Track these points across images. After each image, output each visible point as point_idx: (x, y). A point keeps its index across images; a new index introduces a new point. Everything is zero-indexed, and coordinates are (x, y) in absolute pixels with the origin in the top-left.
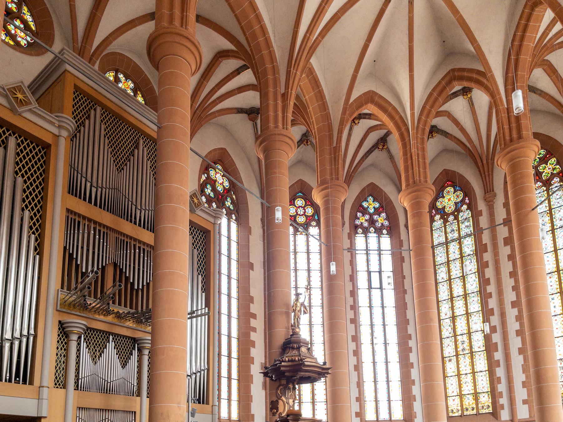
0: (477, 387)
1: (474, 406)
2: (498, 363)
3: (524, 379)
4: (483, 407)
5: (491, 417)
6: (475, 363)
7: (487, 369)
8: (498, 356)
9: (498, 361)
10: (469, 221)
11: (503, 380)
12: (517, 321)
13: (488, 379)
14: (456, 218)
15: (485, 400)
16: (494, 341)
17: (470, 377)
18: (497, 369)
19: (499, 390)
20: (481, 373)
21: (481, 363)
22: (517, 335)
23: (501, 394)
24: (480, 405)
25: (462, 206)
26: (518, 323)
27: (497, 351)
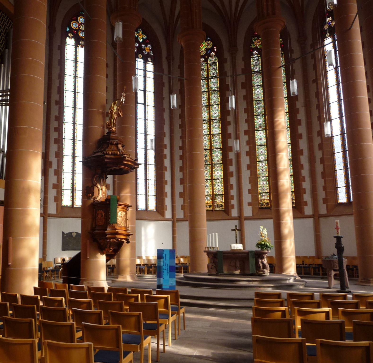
0: (214, 190)
1: (212, 204)
2: (232, 174)
5: (224, 214)
6: (214, 172)
7: (222, 177)
8: (232, 168)
10: (216, 65)
11: (235, 187)
12: (247, 145)
13: (223, 185)
14: (206, 60)
15: (219, 200)
17: (209, 182)
18: (231, 178)
19: (232, 194)
20: (218, 180)
21: (219, 173)
22: (247, 155)
23: (232, 196)
24: (215, 204)
26: (248, 147)
27: (232, 165)
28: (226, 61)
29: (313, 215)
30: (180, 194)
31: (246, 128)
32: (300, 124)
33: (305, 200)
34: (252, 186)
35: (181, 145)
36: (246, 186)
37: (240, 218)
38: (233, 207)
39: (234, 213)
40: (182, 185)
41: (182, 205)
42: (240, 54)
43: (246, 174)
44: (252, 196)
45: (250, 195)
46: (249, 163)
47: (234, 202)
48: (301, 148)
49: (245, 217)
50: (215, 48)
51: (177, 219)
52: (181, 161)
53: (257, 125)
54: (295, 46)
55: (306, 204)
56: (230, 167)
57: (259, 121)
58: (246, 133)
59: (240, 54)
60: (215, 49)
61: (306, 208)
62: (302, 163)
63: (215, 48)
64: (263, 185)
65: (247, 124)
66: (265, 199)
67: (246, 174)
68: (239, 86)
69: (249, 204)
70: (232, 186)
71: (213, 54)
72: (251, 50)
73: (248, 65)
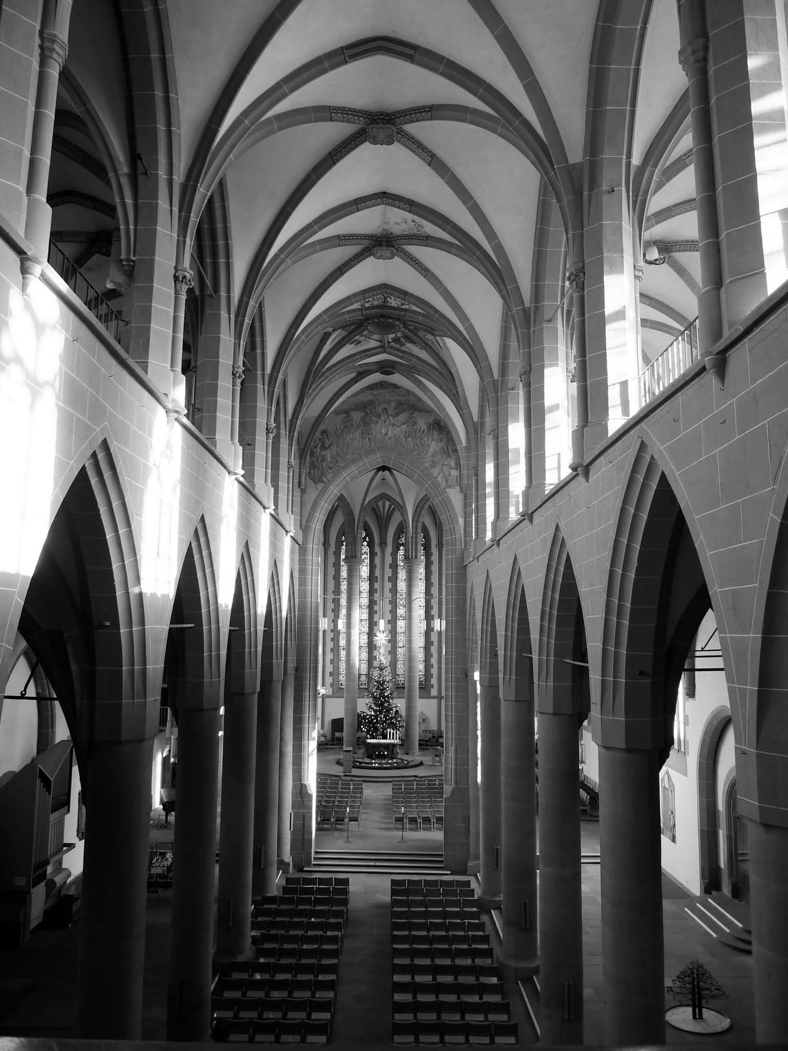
15: (363, 678)
42: (389, 549)
53: (398, 615)
54: (434, 550)
55: (432, 686)
59: (389, 549)
68: (386, 579)
71: (365, 543)
73: (395, 560)
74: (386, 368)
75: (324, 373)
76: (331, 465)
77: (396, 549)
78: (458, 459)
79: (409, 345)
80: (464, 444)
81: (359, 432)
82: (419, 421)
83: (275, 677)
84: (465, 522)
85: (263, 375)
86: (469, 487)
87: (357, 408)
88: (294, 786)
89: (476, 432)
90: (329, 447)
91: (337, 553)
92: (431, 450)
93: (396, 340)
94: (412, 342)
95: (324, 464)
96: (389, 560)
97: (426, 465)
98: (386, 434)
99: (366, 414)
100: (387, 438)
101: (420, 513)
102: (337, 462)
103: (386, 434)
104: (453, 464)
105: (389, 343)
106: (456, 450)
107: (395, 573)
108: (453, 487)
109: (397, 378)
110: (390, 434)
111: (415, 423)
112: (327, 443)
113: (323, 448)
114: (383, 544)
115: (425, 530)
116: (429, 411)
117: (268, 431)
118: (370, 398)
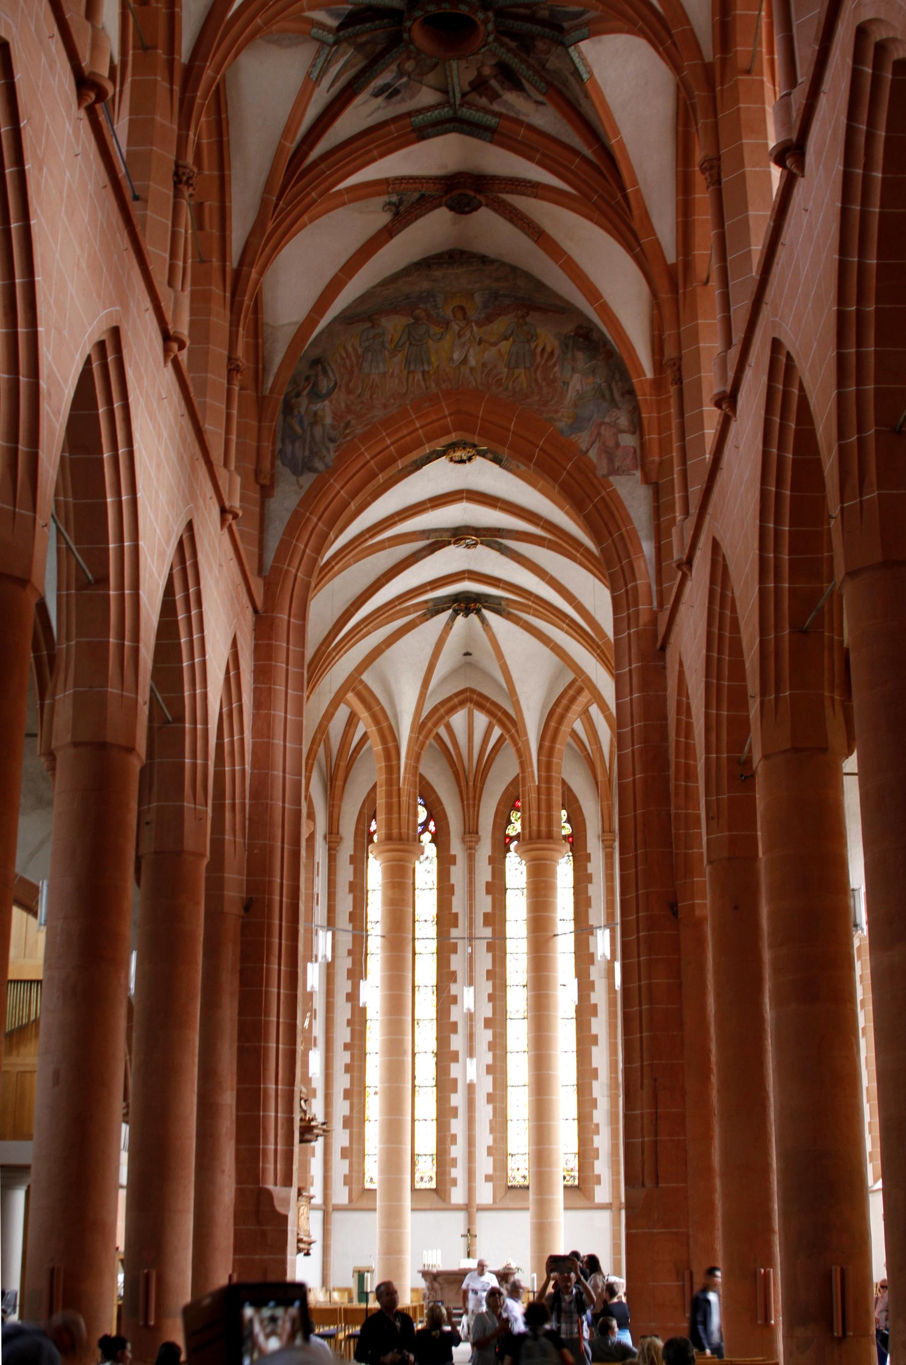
2: (454, 1112)
3: (491, 1144)
4: (422, 1178)
8: (457, 1100)
9: (456, 1109)
11: (461, 1140)
16: (453, 1076)
19: (453, 1155)
23: (454, 1160)
25: (422, 832)
26: (490, 1054)
27: (456, 1091)
28: (453, 860)
29: (611, 1204)
30: (343, 1150)
31: (489, 1014)
32: (595, 1014)
33: (596, 1172)
34: (495, 1140)
35: (348, 1040)
36: (484, 1138)
37: (469, 1208)
38: (454, 1182)
39: (457, 1195)
40: (348, 1131)
41: (345, 1176)
43: (484, 1112)
44: (494, 1161)
45: (491, 1159)
46: (490, 1090)
47: (458, 1173)
48: (594, 1065)
49: (478, 1205)
50: (432, 823)
51: (334, 1205)
52: (348, 1076)
56: (453, 1096)
57: (517, 1000)
58: (488, 1023)
59: (485, 849)
60: (432, 826)
61: (597, 1189)
62: (595, 1095)
63: (432, 823)
64: (519, 1138)
65: (491, 1005)
66: (519, 1168)
67: (484, 1112)
68: (479, 920)
69: (488, 1178)
70: (454, 1137)
71: (426, 837)
72: (508, 840)
73: (499, 873)
74: (463, 191)
75: (315, 164)
76: (333, 433)
77: (502, 845)
78: (636, 410)
79: (510, 97)
80: (649, 374)
81: (400, 357)
82: (540, 331)
83: (189, 844)
84: (659, 550)
85: (171, 63)
86: (665, 466)
87: (393, 309)
88: (240, 1194)
89: (674, 288)
90: (329, 394)
91: (359, 863)
92: (571, 394)
93: (479, 85)
94: (517, 86)
95: (318, 431)
96: (484, 873)
97: (561, 425)
98: (465, 361)
99: (417, 320)
100: (465, 370)
101: (557, 731)
102: (347, 425)
103: (465, 361)
104: (623, 421)
105: (464, 95)
106: (630, 392)
107: (499, 904)
108: (626, 472)
109: (490, 231)
110: (472, 362)
111: (531, 337)
112: (324, 385)
113: (316, 395)
114: (471, 831)
115: (571, 802)
116: (561, 309)
117: (180, 179)
118: (426, 285)
